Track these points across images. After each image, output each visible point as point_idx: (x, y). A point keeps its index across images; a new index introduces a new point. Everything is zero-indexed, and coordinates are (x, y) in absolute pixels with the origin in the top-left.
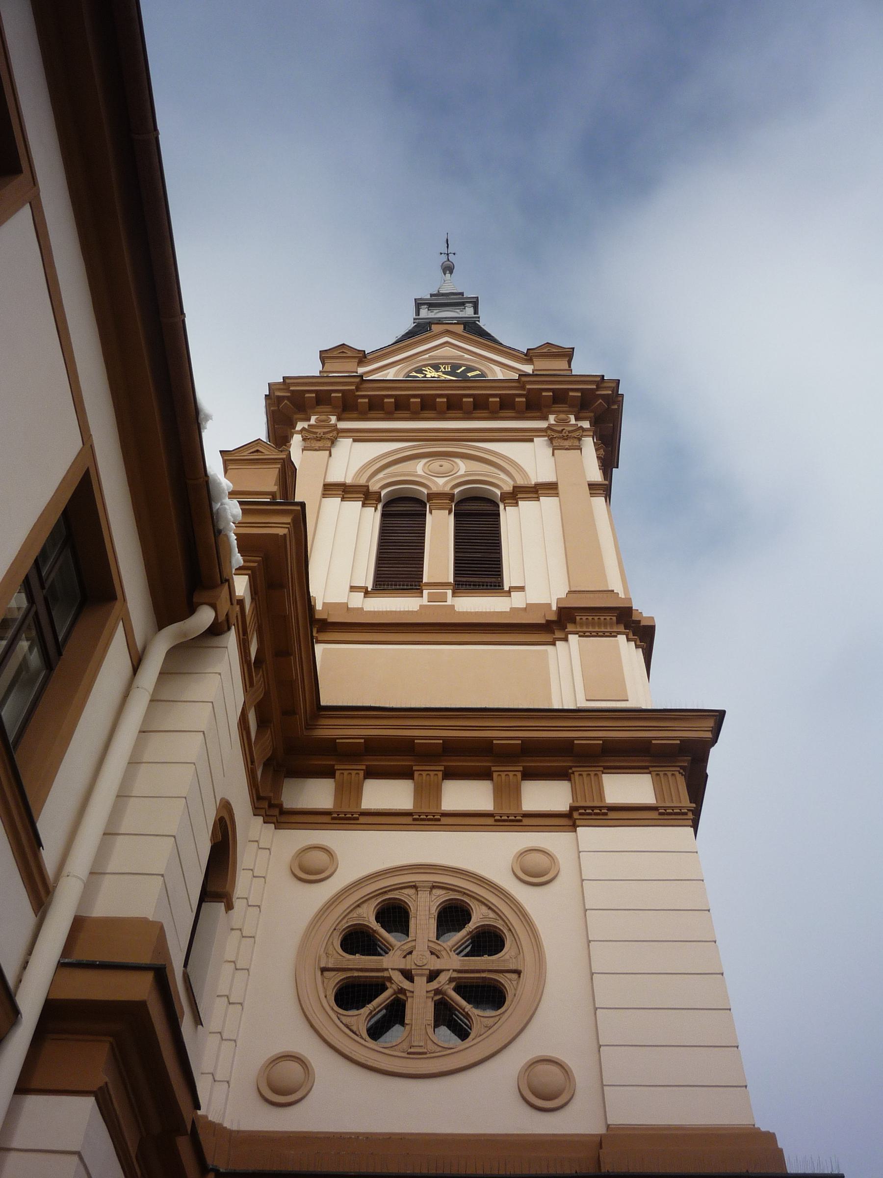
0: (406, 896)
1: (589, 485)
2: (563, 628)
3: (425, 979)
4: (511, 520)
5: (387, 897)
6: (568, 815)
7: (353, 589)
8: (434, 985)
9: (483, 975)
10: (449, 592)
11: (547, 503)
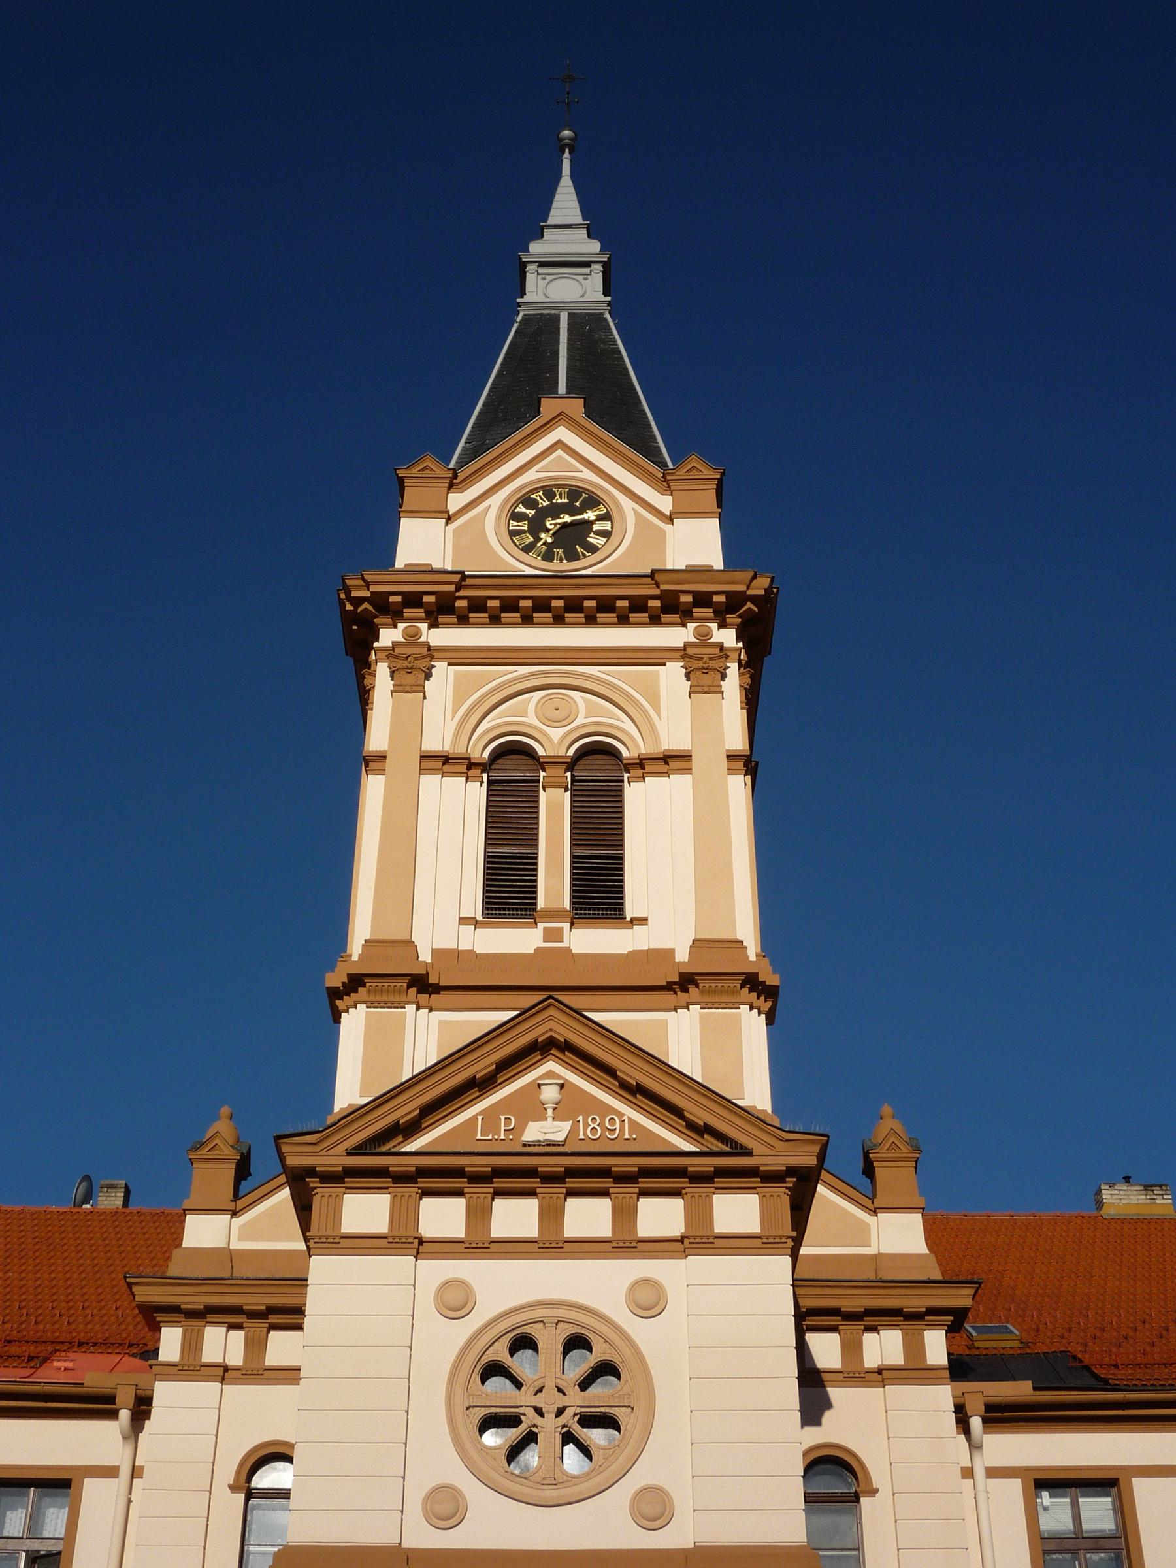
0: (534, 1331)
1: (728, 756)
2: (686, 990)
4: (639, 797)
6: (681, 1240)
7: (463, 921)
8: (562, 1420)
9: (603, 1410)
10: (566, 926)
11: (678, 785)
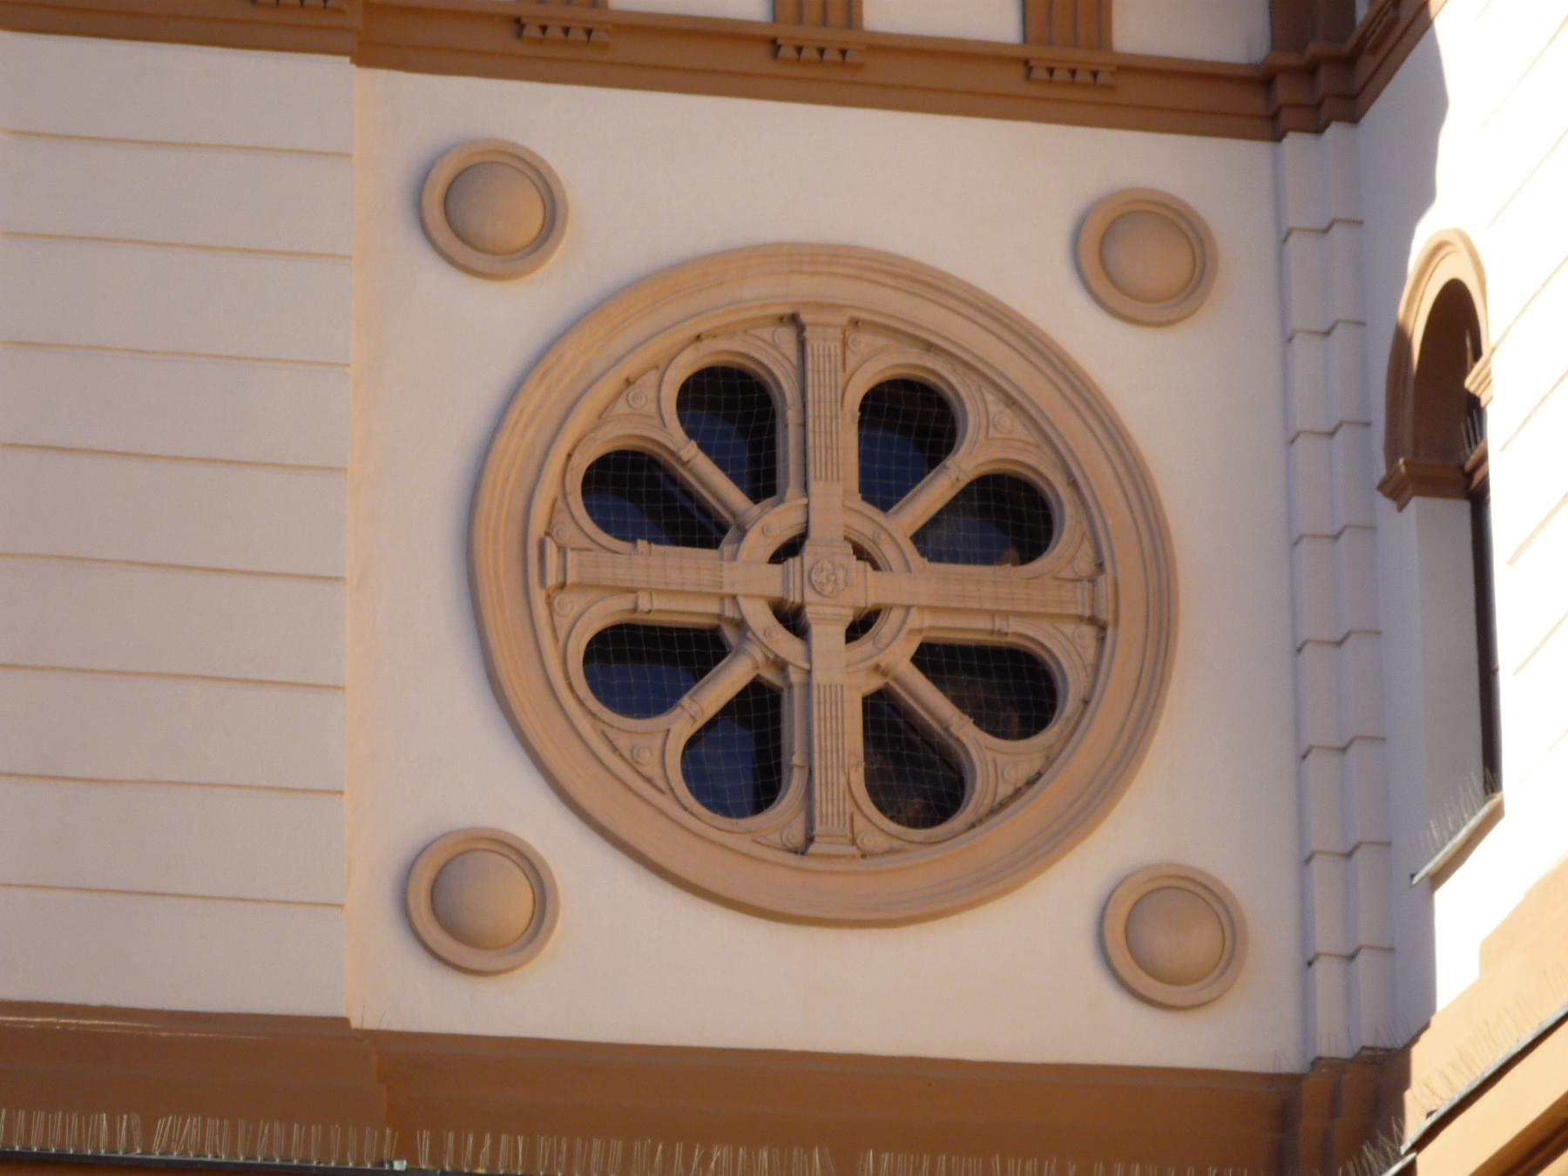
3: (776, 591)
5: (1064, 493)
8: (760, 617)
